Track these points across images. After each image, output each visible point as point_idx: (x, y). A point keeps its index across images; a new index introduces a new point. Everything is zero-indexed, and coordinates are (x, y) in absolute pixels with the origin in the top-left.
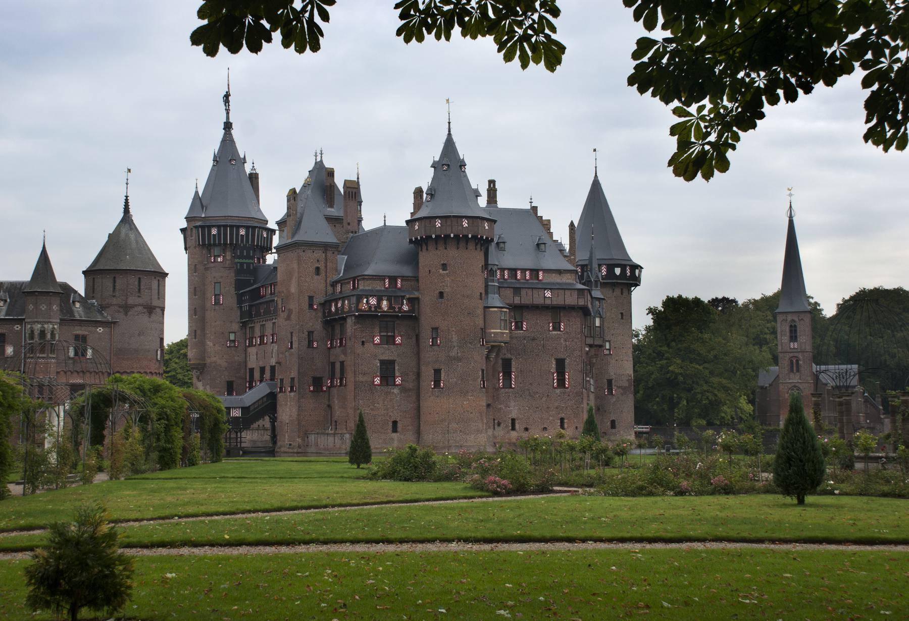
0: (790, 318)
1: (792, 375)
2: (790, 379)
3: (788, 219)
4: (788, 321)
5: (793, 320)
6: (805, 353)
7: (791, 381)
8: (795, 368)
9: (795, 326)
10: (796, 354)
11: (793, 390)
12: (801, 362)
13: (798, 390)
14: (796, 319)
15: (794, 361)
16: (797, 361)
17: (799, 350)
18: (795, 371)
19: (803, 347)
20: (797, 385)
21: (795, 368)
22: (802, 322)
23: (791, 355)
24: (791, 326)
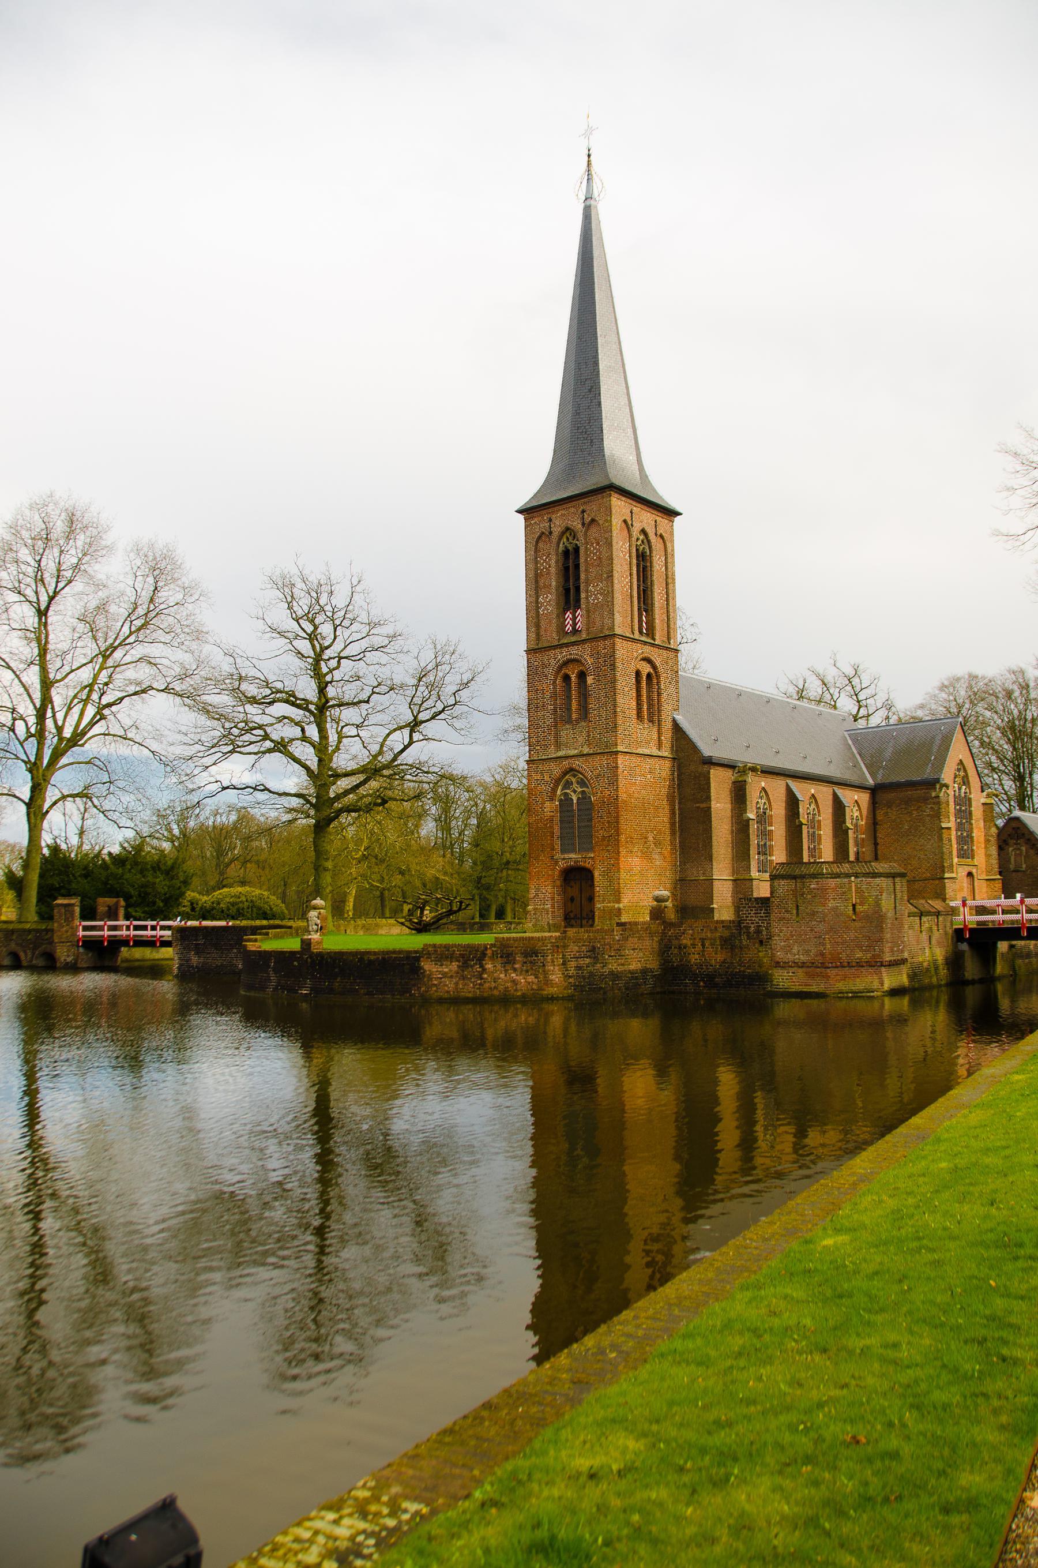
0: (559, 521)
1: (566, 732)
2: (558, 746)
3: (583, 205)
4: (555, 536)
5: (567, 529)
6: (601, 644)
7: (560, 754)
8: (574, 705)
9: (577, 550)
10: (575, 652)
11: (568, 785)
12: (590, 680)
13: (582, 783)
14: (577, 525)
15: (573, 679)
16: (582, 676)
17: (584, 636)
18: (574, 716)
19: (598, 624)
20: (577, 763)
21: (574, 705)
22: (593, 531)
23: (562, 655)
24: (566, 553)
